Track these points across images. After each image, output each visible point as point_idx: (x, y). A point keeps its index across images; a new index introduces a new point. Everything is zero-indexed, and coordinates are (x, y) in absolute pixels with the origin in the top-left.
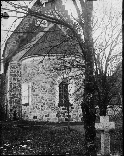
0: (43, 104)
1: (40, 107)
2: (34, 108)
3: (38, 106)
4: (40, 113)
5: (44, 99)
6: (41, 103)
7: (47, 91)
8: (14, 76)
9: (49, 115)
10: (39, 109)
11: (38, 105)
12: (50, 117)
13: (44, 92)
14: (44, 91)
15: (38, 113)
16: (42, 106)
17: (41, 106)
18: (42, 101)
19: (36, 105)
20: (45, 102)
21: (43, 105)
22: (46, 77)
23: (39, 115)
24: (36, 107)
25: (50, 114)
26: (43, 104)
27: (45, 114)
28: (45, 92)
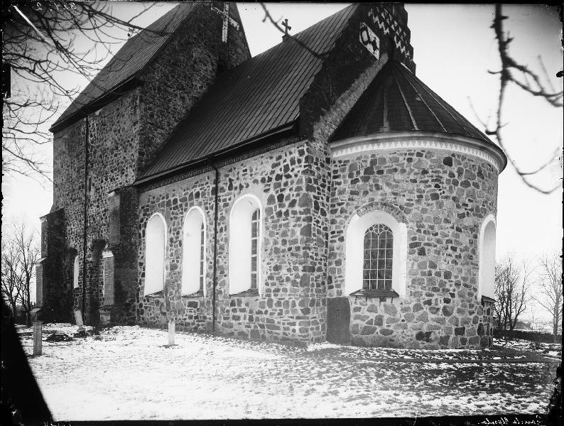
0: (450, 294)
1: (441, 305)
2: (418, 308)
3: (433, 302)
4: (438, 321)
5: (453, 279)
6: (443, 290)
7: (460, 257)
8: (316, 195)
9: (464, 328)
10: (438, 309)
11: (436, 297)
12: (465, 336)
13: (454, 258)
14: (454, 254)
15: (435, 323)
16: (447, 301)
17: (443, 301)
18: (447, 286)
19: (427, 298)
20: (454, 290)
21: (450, 297)
22: (462, 211)
23: (439, 328)
24: (429, 303)
25: (465, 326)
26: (450, 294)
27: (454, 328)
28: (456, 257)
